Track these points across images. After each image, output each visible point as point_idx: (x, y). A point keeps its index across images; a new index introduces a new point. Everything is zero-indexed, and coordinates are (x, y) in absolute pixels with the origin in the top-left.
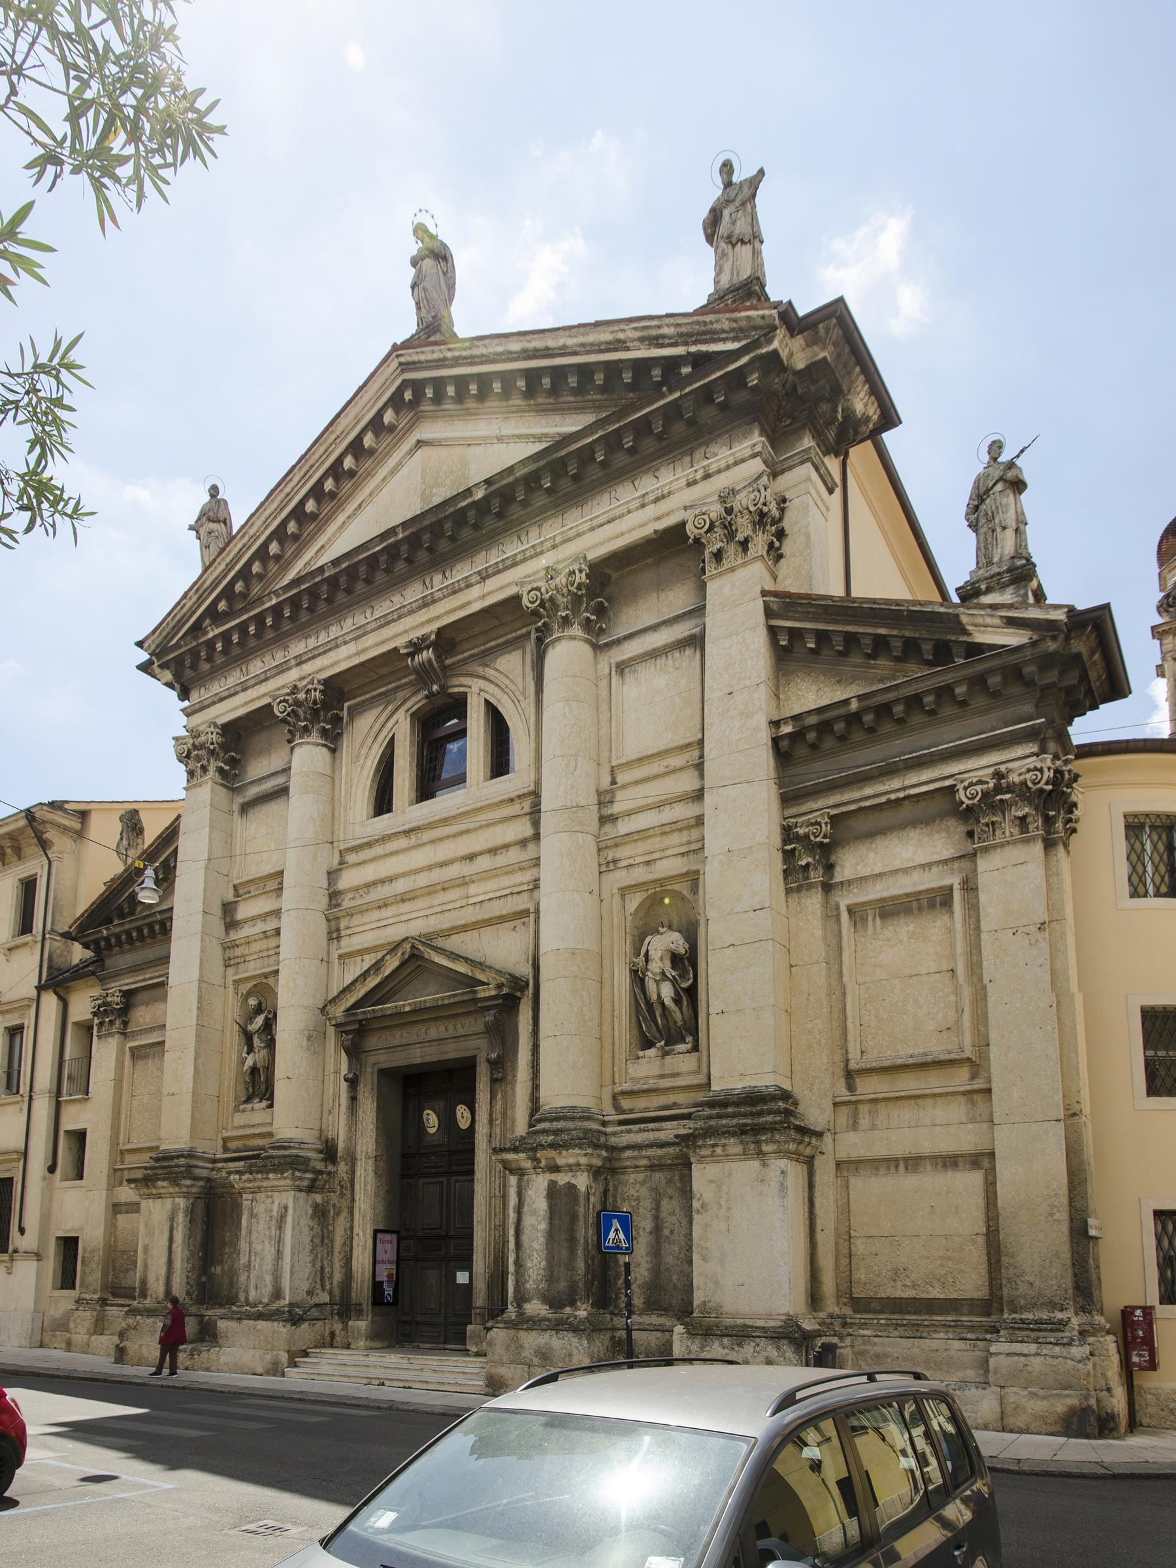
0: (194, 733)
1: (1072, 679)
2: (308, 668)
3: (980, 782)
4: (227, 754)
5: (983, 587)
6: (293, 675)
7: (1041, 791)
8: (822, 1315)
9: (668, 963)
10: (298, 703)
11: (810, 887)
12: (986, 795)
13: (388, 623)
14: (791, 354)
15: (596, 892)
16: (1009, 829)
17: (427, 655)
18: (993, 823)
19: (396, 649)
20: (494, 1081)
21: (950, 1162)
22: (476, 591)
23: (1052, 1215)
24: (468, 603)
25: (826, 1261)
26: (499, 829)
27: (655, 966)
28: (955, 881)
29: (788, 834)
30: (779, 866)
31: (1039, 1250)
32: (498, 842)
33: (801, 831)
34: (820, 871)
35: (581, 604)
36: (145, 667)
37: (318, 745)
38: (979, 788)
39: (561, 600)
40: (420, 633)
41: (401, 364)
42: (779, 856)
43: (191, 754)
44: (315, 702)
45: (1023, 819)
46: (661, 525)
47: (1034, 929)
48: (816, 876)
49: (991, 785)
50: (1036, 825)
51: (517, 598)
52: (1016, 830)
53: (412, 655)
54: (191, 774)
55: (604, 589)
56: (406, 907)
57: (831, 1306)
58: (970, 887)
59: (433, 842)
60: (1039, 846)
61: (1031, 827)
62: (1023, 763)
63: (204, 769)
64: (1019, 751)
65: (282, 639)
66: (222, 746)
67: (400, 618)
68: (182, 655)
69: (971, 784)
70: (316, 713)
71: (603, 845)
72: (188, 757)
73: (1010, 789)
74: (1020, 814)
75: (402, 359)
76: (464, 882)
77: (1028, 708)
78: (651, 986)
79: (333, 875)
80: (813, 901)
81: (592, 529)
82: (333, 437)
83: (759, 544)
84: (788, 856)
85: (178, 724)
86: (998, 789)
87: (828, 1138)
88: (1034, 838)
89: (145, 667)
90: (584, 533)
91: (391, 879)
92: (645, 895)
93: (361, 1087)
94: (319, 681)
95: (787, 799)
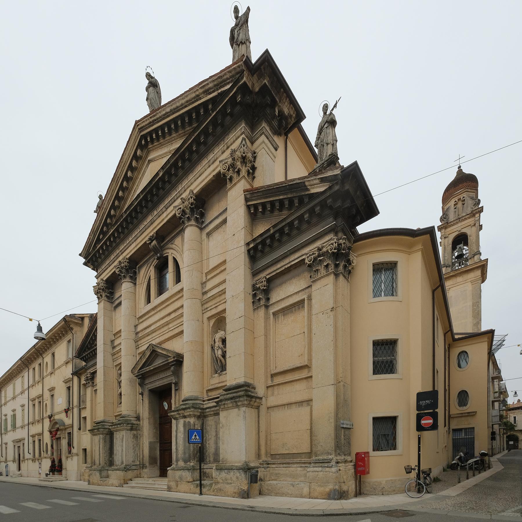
0: (98, 284)
1: (347, 204)
2: (124, 254)
3: (313, 254)
4: (107, 290)
5: (318, 171)
6: (120, 258)
7: (333, 252)
8: (261, 461)
9: (221, 343)
10: (122, 268)
11: (261, 306)
12: (315, 259)
13: (143, 233)
14: (253, 85)
15: (200, 320)
16: (323, 271)
17: (154, 242)
18: (317, 270)
19: (146, 242)
20: (176, 390)
21: (300, 403)
22: (165, 215)
23: (329, 420)
24: (163, 220)
25: (263, 443)
26: (176, 303)
27: (217, 345)
28: (305, 297)
29: (254, 288)
30: (251, 300)
31: (326, 432)
32: (176, 307)
33: (258, 286)
34: (264, 300)
35: (194, 212)
36: (85, 264)
37: (129, 282)
38: (312, 256)
39: (188, 211)
40: (151, 234)
41: (139, 129)
42: (251, 297)
43: (98, 291)
44: (126, 267)
45: (327, 266)
46: (214, 173)
47: (329, 310)
48: (262, 302)
49: (317, 254)
50: (332, 268)
51: (175, 215)
52: (325, 272)
53: (150, 243)
54: (98, 298)
55: (201, 204)
56: (154, 335)
57: (264, 458)
58: (310, 298)
59: (159, 311)
60: (332, 277)
61: (330, 269)
62: (329, 242)
63: (101, 295)
64: (327, 238)
65: (118, 245)
66: (106, 288)
67: (146, 230)
68: (93, 256)
69: (310, 255)
70: (127, 270)
71: (203, 303)
72: (97, 293)
73: (323, 255)
74: (325, 264)
75: (139, 127)
76: (167, 323)
77: (331, 219)
78: (216, 351)
79: (136, 326)
80: (262, 312)
81: (195, 180)
82: (123, 164)
83: (244, 172)
84: (254, 296)
85: (94, 282)
86: (319, 256)
87: (264, 399)
88: (331, 273)
89: (85, 264)
90: (193, 183)
91: (150, 326)
92: (215, 319)
93: (144, 396)
94: (127, 259)
95: (255, 274)
